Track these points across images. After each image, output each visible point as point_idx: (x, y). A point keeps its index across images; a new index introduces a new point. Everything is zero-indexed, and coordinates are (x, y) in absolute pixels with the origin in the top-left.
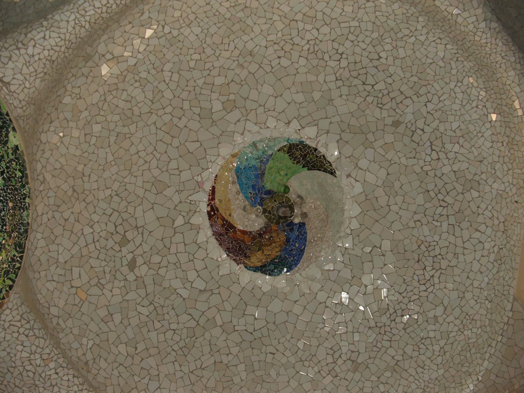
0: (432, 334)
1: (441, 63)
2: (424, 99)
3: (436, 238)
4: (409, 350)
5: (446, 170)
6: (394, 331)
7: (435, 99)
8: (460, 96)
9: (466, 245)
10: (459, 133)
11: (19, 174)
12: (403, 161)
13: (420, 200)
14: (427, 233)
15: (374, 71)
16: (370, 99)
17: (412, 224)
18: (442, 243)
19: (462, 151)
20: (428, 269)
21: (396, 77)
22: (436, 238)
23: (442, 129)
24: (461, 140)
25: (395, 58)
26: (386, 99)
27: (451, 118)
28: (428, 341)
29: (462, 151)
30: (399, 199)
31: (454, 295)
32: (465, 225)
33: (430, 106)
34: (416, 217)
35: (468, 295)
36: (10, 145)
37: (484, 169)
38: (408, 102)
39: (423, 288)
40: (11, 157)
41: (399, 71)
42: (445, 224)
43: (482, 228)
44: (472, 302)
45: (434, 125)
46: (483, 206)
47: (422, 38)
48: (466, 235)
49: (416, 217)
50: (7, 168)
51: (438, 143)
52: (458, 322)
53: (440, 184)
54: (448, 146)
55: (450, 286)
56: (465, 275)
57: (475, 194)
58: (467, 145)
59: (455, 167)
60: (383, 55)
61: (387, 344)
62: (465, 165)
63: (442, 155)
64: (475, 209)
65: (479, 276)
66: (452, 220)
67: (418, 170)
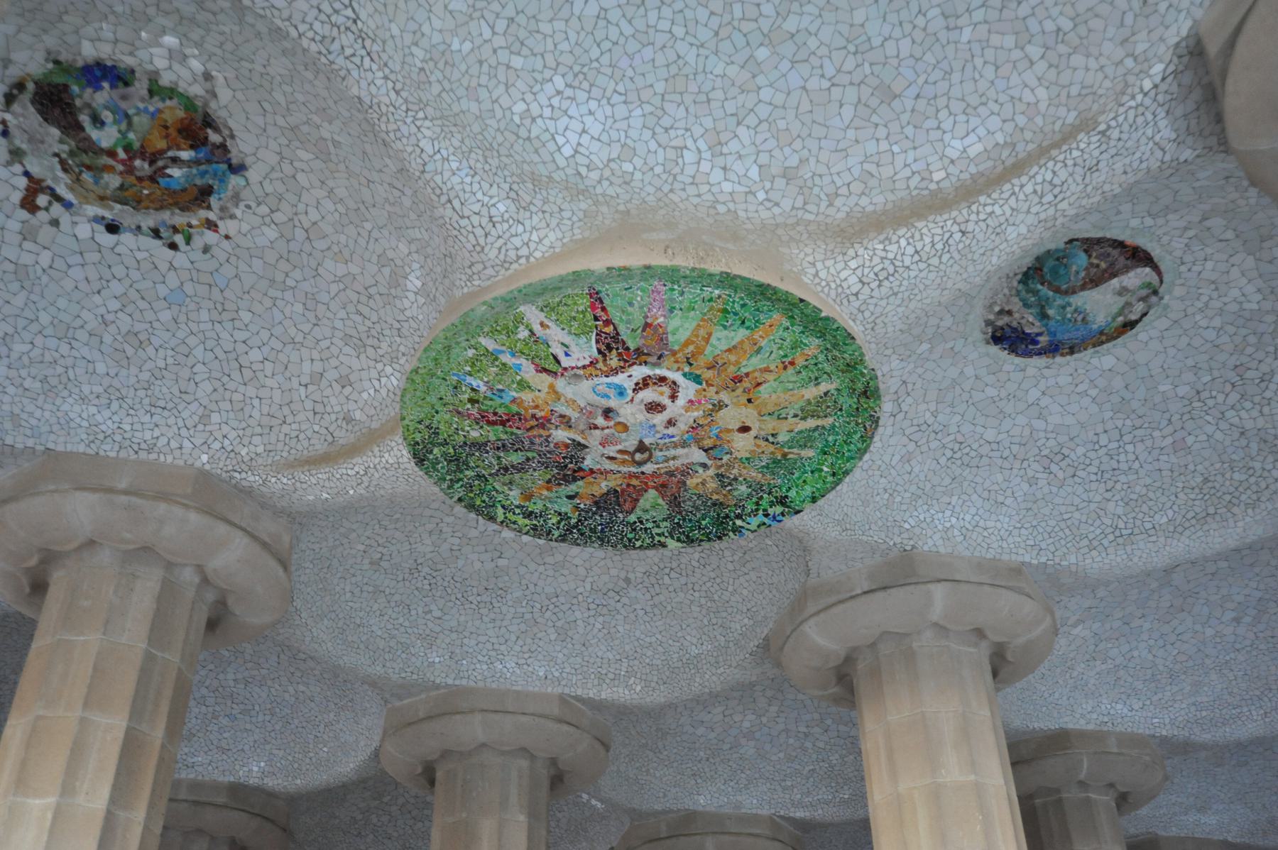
0: (413, 612)
1: (680, 634)
2: (649, 609)
3: (510, 603)
4: (397, 597)
5: (578, 614)
6: (414, 581)
7: (647, 619)
8: (648, 639)
9: (503, 630)
10: (613, 630)
11: (638, 544)
12: (590, 579)
13: (549, 590)
14: (516, 595)
15: (683, 580)
16: (656, 568)
17: (524, 582)
18: (504, 609)
19: (596, 631)
20: (479, 598)
21: (673, 595)
22: (510, 603)
23: (618, 617)
24: (605, 631)
25: (692, 602)
26: (653, 580)
27: (627, 627)
28: (406, 611)
29: (596, 631)
30: (551, 573)
31: (454, 623)
32: (523, 627)
33: (641, 613)
34: (531, 587)
35: (454, 636)
36: (669, 541)
37: (577, 647)
38: (648, 596)
39: (459, 596)
40: (657, 538)
41: (678, 599)
42: (523, 610)
43: (520, 642)
44: (447, 641)
45: (622, 611)
46: (541, 643)
47: (706, 630)
48: (514, 628)
49: (531, 587)
50: (646, 529)
51: (605, 611)
52: (428, 632)
53: (565, 608)
54: (601, 619)
55: (462, 619)
56: (473, 630)
57: (553, 637)
58: (600, 635)
59: (580, 622)
60: (697, 594)
61: (400, 578)
62: (581, 631)
63: (592, 613)
64: (539, 635)
65: (473, 642)
66: (528, 616)
67: (579, 590)
